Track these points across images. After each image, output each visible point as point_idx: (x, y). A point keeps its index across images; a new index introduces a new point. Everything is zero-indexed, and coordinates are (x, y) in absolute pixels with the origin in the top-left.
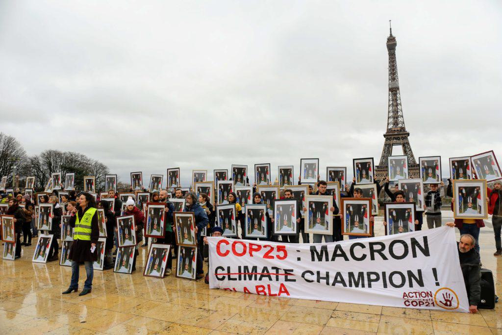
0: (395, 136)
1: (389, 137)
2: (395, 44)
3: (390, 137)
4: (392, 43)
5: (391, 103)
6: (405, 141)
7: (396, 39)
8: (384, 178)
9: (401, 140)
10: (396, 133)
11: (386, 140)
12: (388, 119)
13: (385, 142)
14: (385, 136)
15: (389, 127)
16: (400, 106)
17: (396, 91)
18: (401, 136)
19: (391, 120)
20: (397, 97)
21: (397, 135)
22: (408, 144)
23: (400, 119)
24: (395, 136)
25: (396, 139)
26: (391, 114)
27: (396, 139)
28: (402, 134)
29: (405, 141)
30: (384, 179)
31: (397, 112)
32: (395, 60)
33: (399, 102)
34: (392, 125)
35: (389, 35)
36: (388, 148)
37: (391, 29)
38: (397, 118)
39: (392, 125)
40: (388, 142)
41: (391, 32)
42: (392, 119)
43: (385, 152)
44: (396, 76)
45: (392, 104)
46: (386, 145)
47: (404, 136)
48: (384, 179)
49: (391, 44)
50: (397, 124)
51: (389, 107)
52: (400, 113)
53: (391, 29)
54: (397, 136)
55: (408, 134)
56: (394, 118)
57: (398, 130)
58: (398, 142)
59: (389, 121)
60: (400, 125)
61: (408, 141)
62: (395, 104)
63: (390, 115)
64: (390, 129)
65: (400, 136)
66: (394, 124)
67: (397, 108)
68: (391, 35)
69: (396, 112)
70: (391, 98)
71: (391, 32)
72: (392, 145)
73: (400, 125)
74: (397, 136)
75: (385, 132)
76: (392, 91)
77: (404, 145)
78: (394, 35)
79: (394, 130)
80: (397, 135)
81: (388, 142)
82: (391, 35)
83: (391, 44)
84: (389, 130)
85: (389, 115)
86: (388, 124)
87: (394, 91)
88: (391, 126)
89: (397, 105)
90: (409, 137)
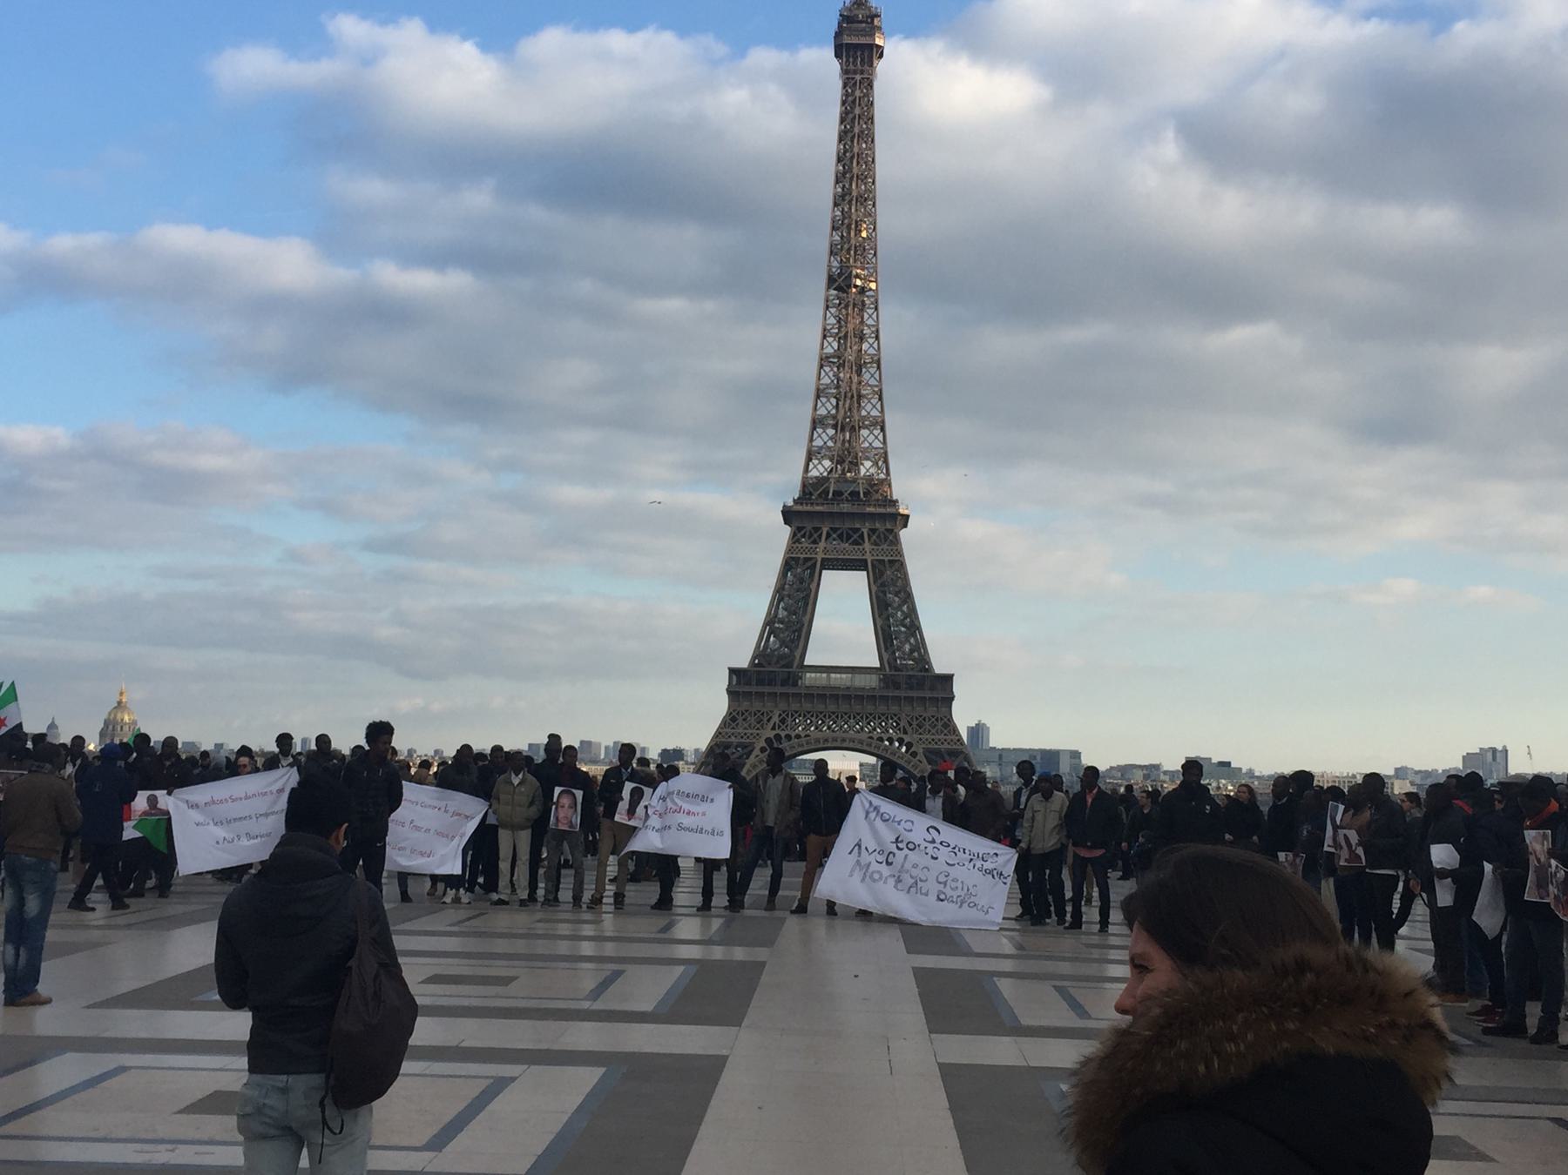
4: (863, 41)
5: (832, 346)
8: (771, 734)
9: (867, 546)
10: (846, 507)
11: (794, 535)
12: (814, 429)
13: (789, 550)
14: (788, 515)
15: (814, 473)
19: (824, 437)
21: (844, 520)
22: (899, 565)
23: (868, 438)
25: (845, 537)
26: (827, 407)
27: (840, 537)
28: (872, 515)
31: (860, 396)
36: (802, 581)
39: (827, 463)
42: (831, 432)
45: (838, 355)
46: (788, 564)
50: (855, 465)
52: (869, 409)
54: (848, 525)
57: (855, 495)
58: (847, 550)
60: (866, 468)
61: (900, 553)
62: (850, 356)
63: (822, 412)
64: (821, 481)
69: (849, 397)
72: (823, 567)
73: (866, 468)
76: (838, 289)
80: (844, 520)
84: (810, 489)
88: (820, 468)
90: (903, 534)
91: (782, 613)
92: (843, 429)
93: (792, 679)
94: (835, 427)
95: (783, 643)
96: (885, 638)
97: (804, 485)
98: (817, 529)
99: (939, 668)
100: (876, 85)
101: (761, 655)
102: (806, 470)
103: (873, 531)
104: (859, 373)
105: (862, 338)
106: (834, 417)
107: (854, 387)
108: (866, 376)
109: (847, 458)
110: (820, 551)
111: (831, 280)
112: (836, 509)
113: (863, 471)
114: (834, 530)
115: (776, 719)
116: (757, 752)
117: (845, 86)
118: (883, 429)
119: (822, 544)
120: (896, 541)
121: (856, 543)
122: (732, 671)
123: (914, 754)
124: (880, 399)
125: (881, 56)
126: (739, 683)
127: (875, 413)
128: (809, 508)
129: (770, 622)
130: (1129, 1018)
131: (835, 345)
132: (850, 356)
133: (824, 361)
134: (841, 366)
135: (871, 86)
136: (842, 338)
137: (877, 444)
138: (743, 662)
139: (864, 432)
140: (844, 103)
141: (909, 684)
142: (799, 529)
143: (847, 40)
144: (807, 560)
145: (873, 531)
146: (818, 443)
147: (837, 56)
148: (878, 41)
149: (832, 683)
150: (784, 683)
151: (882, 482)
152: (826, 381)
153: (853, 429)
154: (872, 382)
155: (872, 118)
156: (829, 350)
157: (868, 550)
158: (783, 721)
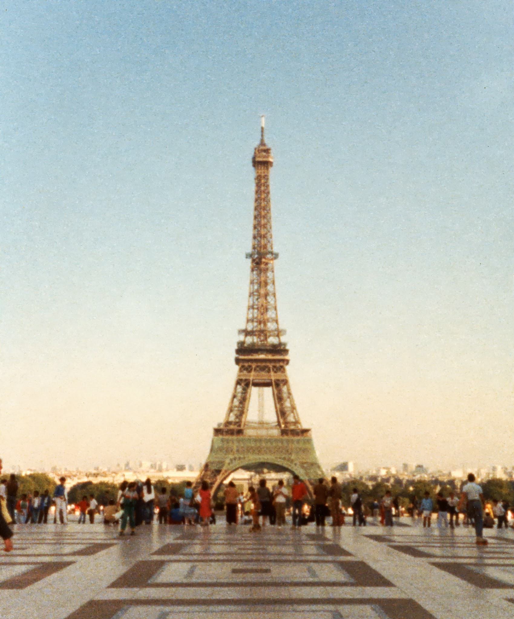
0: (259, 364)
1: (246, 365)
3: (250, 364)
4: (265, 159)
11: (241, 370)
13: (239, 376)
16: (272, 297)
18: (273, 364)
20: (267, 277)
22: (285, 382)
24: (259, 364)
30: (231, 460)
31: (267, 310)
37: (262, 128)
40: (245, 375)
41: (262, 135)
45: (257, 291)
48: (231, 460)
52: (270, 314)
56: (260, 322)
58: (264, 376)
61: (286, 376)
62: (262, 292)
65: (271, 365)
70: (255, 277)
73: (272, 340)
74: (264, 364)
81: (245, 375)
89: (266, 295)
90: (288, 368)
93: (240, 432)
94: (257, 322)
96: (282, 413)
98: (250, 366)
99: (305, 426)
103: (274, 367)
104: (266, 299)
106: (256, 318)
107: (264, 305)
110: (252, 376)
114: (258, 366)
116: (226, 465)
123: (296, 464)
125: (272, 166)
127: (273, 316)
130: (330, 485)
132: (262, 292)
133: (251, 294)
134: (259, 296)
135: (267, 179)
136: (260, 284)
141: (292, 432)
142: (243, 366)
143: (258, 159)
144: (246, 380)
145: (274, 367)
147: (254, 166)
148: (271, 160)
157: (273, 376)
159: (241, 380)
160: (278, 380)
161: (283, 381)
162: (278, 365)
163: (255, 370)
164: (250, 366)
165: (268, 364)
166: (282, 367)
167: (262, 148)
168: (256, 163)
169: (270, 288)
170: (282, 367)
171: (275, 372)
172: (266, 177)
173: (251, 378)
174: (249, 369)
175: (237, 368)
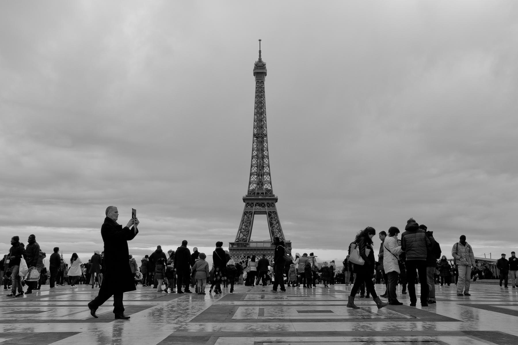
1: (250, 202)
2: (265, 74)
5: (255, 153)
6: (271, 209)
7: (267, 67)
8: (241, 261)
9: (266, 207)
10: (260, 197)
11: (246, 206)
12: (251, 175)
13: (245, 209)
14: (244, 200)
15: (251, 188)
17: (263, 138)
19: (254, 178)
20: (263, 146)
21: (261, 200)
22: (275, 213)
23: (266, 178)
24: (258, 202)
25: (260, 205)
26: (255, 170)
27: (259, 205)
29: (271, 209)
31: (263, 167)
32: (264, 95)
33: (266, 154)
34: (255, 185)
35: (258, 60)
36: (248, 218)
37: (260, 52)
38: (262, 175)
39: (255, 185)
41: (260, 56)
42: (256, 176)
43: (243, 223)
44: (264, 117)
45: (257, 155)
46: (245, 213)
47: (270, 202)
49: (260, 71)
50: (262, 185)
51: (252, 159)
52: (266, 170)
53: (260, 52)
54: (262, 202)
55: (276, 200)
56: (258, 175)
57: (263, 193)
59: (252, 179)
61: (275, 209)
62: (260, 156)
63: (253, 171)
64: (253, 190)
66: (258, 184)
67: (263, 162)
68: (260, 59)
70: (255, 146)
71: (260, 56)
72: (254, 214)
74: (262, 202)
75: (245, 193)
76: (257, 138)
77: (269, 215)
78: (264, 60)
79: (258, 193)
80: (261, 200)
81: (249, 209)
82: (260, 59)
83: (260, 71)
84: (251, 193)
85: (251, 170)
86: (250, 183)
87: (260, 136)
88: (253, 186)
89: (263, 157)
90: (276, 204)
91: (244, 227)
92: (259, 176)
94: (257, 175)
95: (244, 235)
96: (272, 233)
97: (249, 191)
100: (265, 83)
101: (238, 238)
102: (249, 187)
103: (268, 203)
104: (263, 161)
105: (263, 151)
108: (265, 161)
109: (260, 183)
111: (254, 135)
112: (257, 198)
113: (264, 187)
114: (257, 203)
115: (243, 256)
117: (257, 83)
118: (270, 175)
119: (254, 207)
120: (274, 206)
121: (263, 207)
122: (230, 243)
124: (269, 167)
126: (232, 246)
127: (267, 171)
128: (250, 198)
129: (240, 230)
131: (256, 153)
137: (268, 179)
138: (233, 241)
139: (265, 176)
140: (256, 88)
142: (248, 203)
146: (252, 179)
149: (258, 246)
150: (245, 246)
151: (270, 190)
152: (254, 162)
153: (261, 176)
154: (267, 162)
155: (264, 92)
156: (254, 154)
157: (267, 209)
158: (245, 257)
159: (247, 212)
160: (271, 212)
161: (273, 212)
162: (270, 202)
163: (256, 205)
164: (252, 203)
165: (264, 202)
166: (273, 203)
167: (260, 64)
168: (255, 74)
169: (265, 153)
170: (273, 203)
171: (268, 207)
172: (263, 82)
173: (253, 211)
174: (251, 205)
175: (244, 204)
